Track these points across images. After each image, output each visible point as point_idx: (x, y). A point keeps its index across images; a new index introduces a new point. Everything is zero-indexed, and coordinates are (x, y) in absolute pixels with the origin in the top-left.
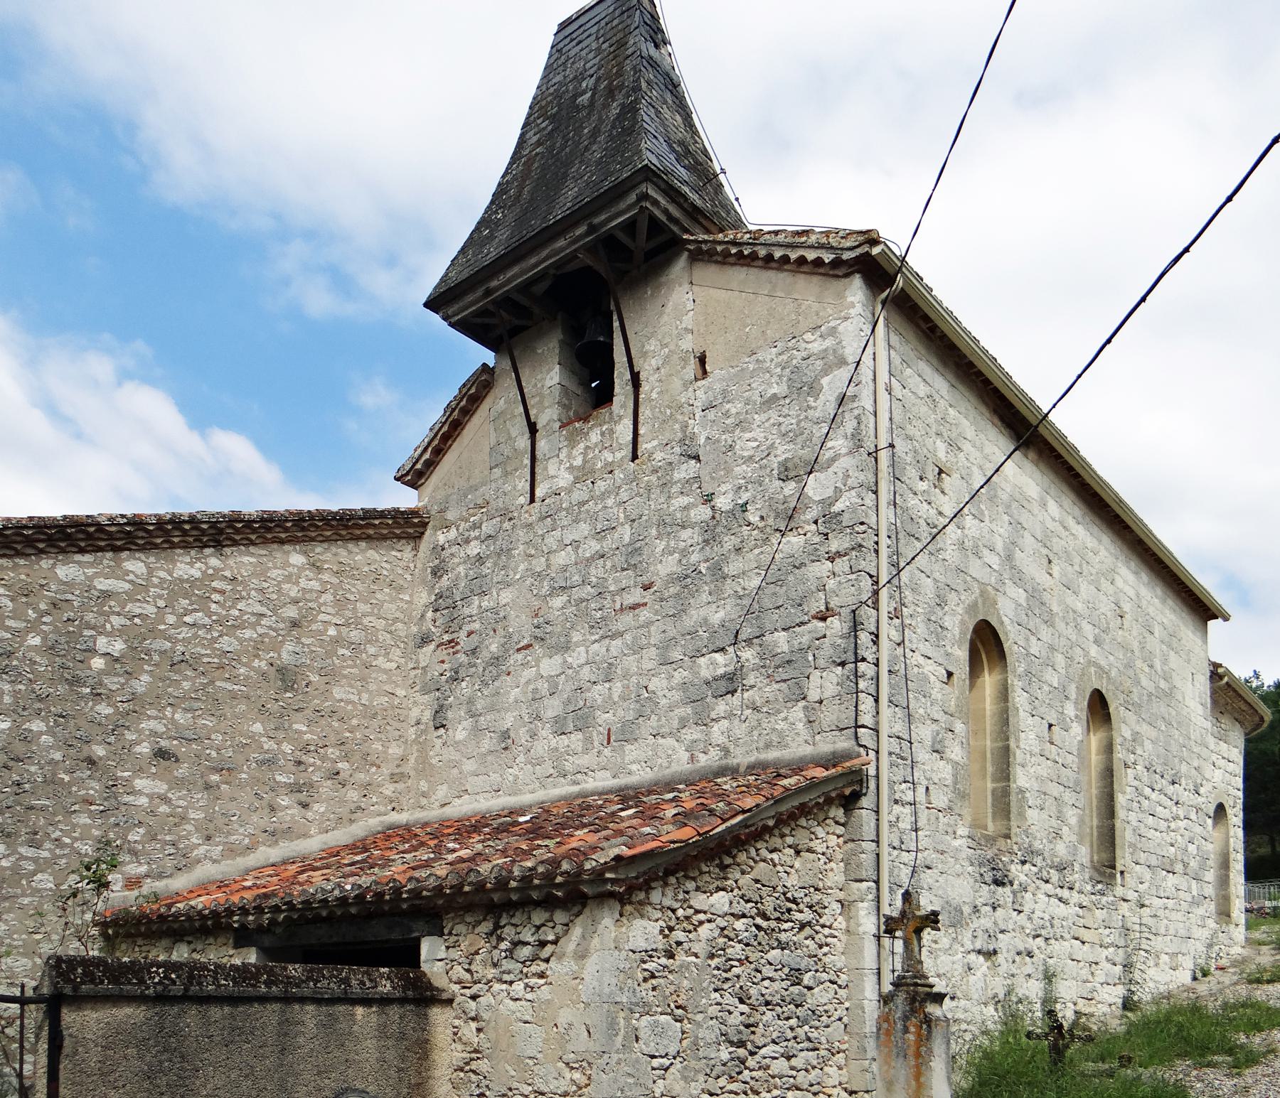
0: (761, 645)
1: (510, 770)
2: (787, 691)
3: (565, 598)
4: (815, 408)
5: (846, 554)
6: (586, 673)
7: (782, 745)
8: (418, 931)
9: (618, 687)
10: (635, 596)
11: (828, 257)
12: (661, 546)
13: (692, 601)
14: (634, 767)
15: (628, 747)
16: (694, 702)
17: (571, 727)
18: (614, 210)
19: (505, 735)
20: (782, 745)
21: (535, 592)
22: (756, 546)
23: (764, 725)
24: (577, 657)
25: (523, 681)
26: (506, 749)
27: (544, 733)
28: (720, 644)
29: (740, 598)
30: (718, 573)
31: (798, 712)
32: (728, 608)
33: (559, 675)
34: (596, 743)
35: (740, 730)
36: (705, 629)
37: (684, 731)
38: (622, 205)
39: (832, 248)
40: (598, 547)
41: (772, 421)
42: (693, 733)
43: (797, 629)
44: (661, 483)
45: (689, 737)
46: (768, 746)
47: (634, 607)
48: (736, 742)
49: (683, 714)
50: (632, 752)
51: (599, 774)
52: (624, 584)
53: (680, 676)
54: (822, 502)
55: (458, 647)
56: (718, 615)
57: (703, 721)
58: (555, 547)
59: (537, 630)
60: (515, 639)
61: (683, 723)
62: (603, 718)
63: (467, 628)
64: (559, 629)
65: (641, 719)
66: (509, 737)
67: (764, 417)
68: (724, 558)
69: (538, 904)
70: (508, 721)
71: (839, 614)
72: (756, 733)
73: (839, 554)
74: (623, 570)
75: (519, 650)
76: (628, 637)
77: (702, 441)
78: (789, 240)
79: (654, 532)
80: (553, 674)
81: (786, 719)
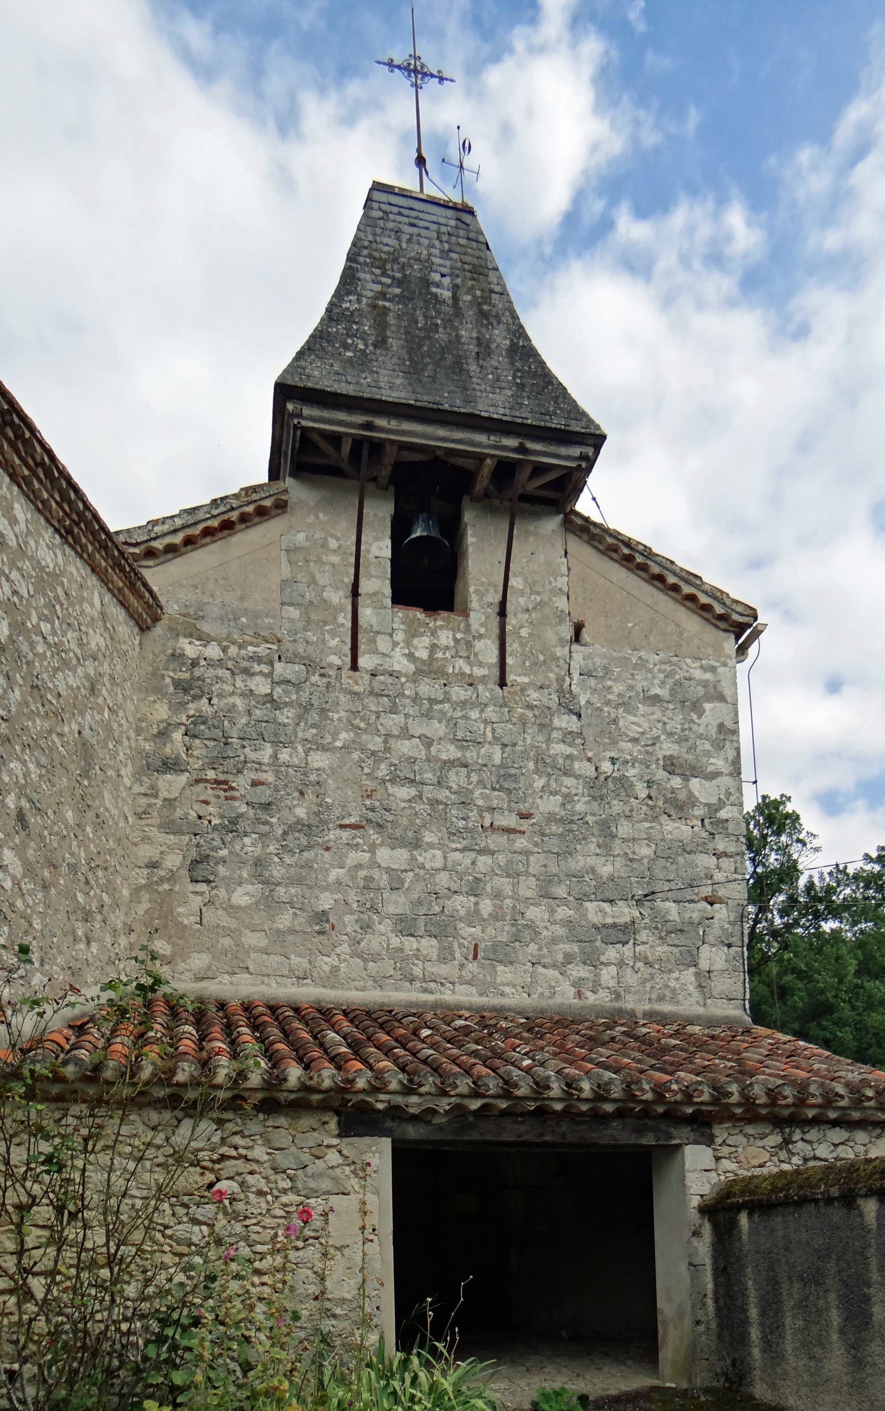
0: (652, 909)
1: (326, 959)
2: (678, 955)
3: (413, 792)
4: (699, 725)
5: (731, 857)
6: (443, 878)
7: (674, 1000)
8: (681, 1138)
9: (486, 906)
10: (511, 820)
11: (719, 610)
12: (539, 783)
13: (578, 847)
14: (507, 990)
15: (500, 968)
16: (581, 941)
17: (421, 931)
18: (552, 449)
19: (321, 917)
20: (674, 1000)
21: (366, 770)
22: (645, 820)
23: (658, 980)
24: (432, 858)
25: (349, 863)
26: (321, 933)
27: (381, 928)
28: (608, 895)
29: (631, 860)
30: (606, 829)
31: (688, 976)
32: (618, 865)
33: (406, 871)
34: (458, 955)
35: (631, 979)
36: (591, 877)
37: (570, 966)
38: (563, 451)
39: (724, 604)
40: (459, 755)
41: (655, 717)
42: (579, 971)
43: (686, 904)
44: (538, 721)
45: (575, 973)
46: (661, 999)
47: (508, 831)
48: (628, 990)
49: (569, 950)
50: (504, 973)
51: (459, 988)
52: (495, 803)
53: (563, 912)
54: (708, 805)
55: (236, 794)
56: (605, 869)
57: (592, 960)
58: (396, 733)
59: (370, 813)
60: (337, 812)
61: (569, 959)
62: (469, 932)
63: (250, 775)
64: (405, 822)
65: (517, 944)
66: (328, 921)
67: (650, 709)
68: (616, 819)
69: (835, 1124)
70: (326, 901)
71: (727, 903)
72: (648, 985)
73: (725, 854)
74: (494, 789)
75: (342, 826)
76: (502, 859)
77: (583, 703)
78: (686, 576)
79: (531, 766)
80: (394, 867)
81: (677, 979)
